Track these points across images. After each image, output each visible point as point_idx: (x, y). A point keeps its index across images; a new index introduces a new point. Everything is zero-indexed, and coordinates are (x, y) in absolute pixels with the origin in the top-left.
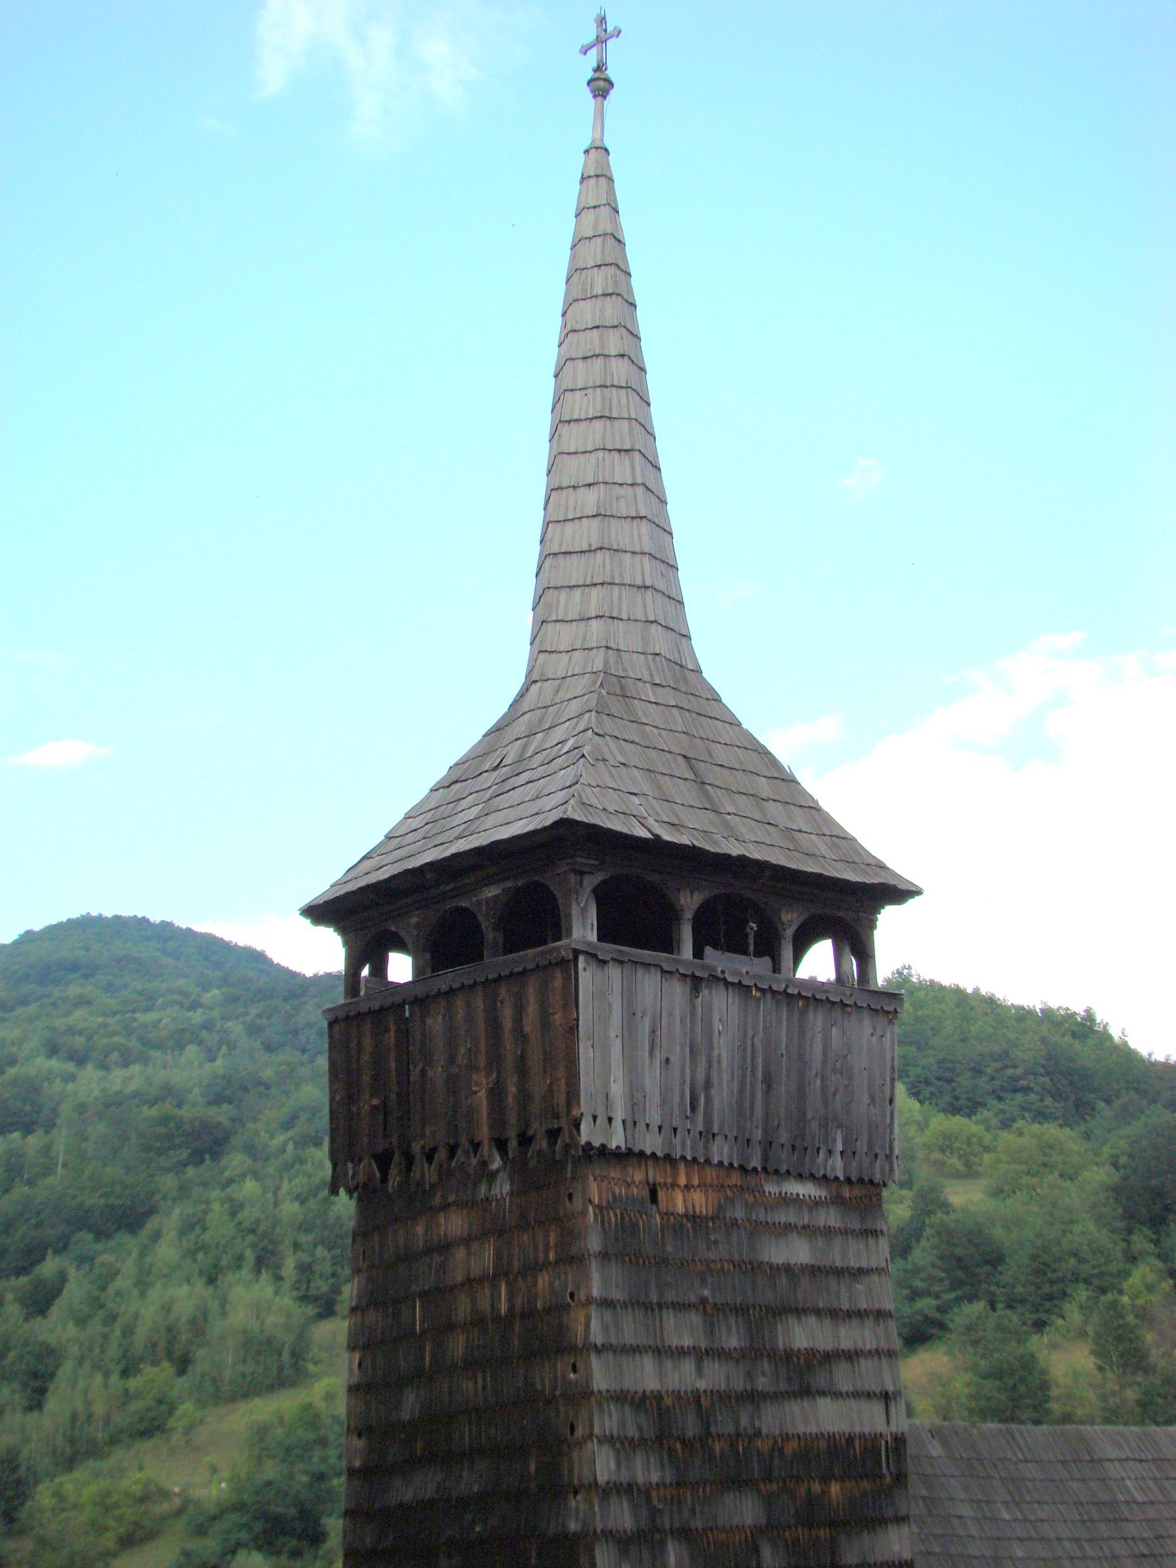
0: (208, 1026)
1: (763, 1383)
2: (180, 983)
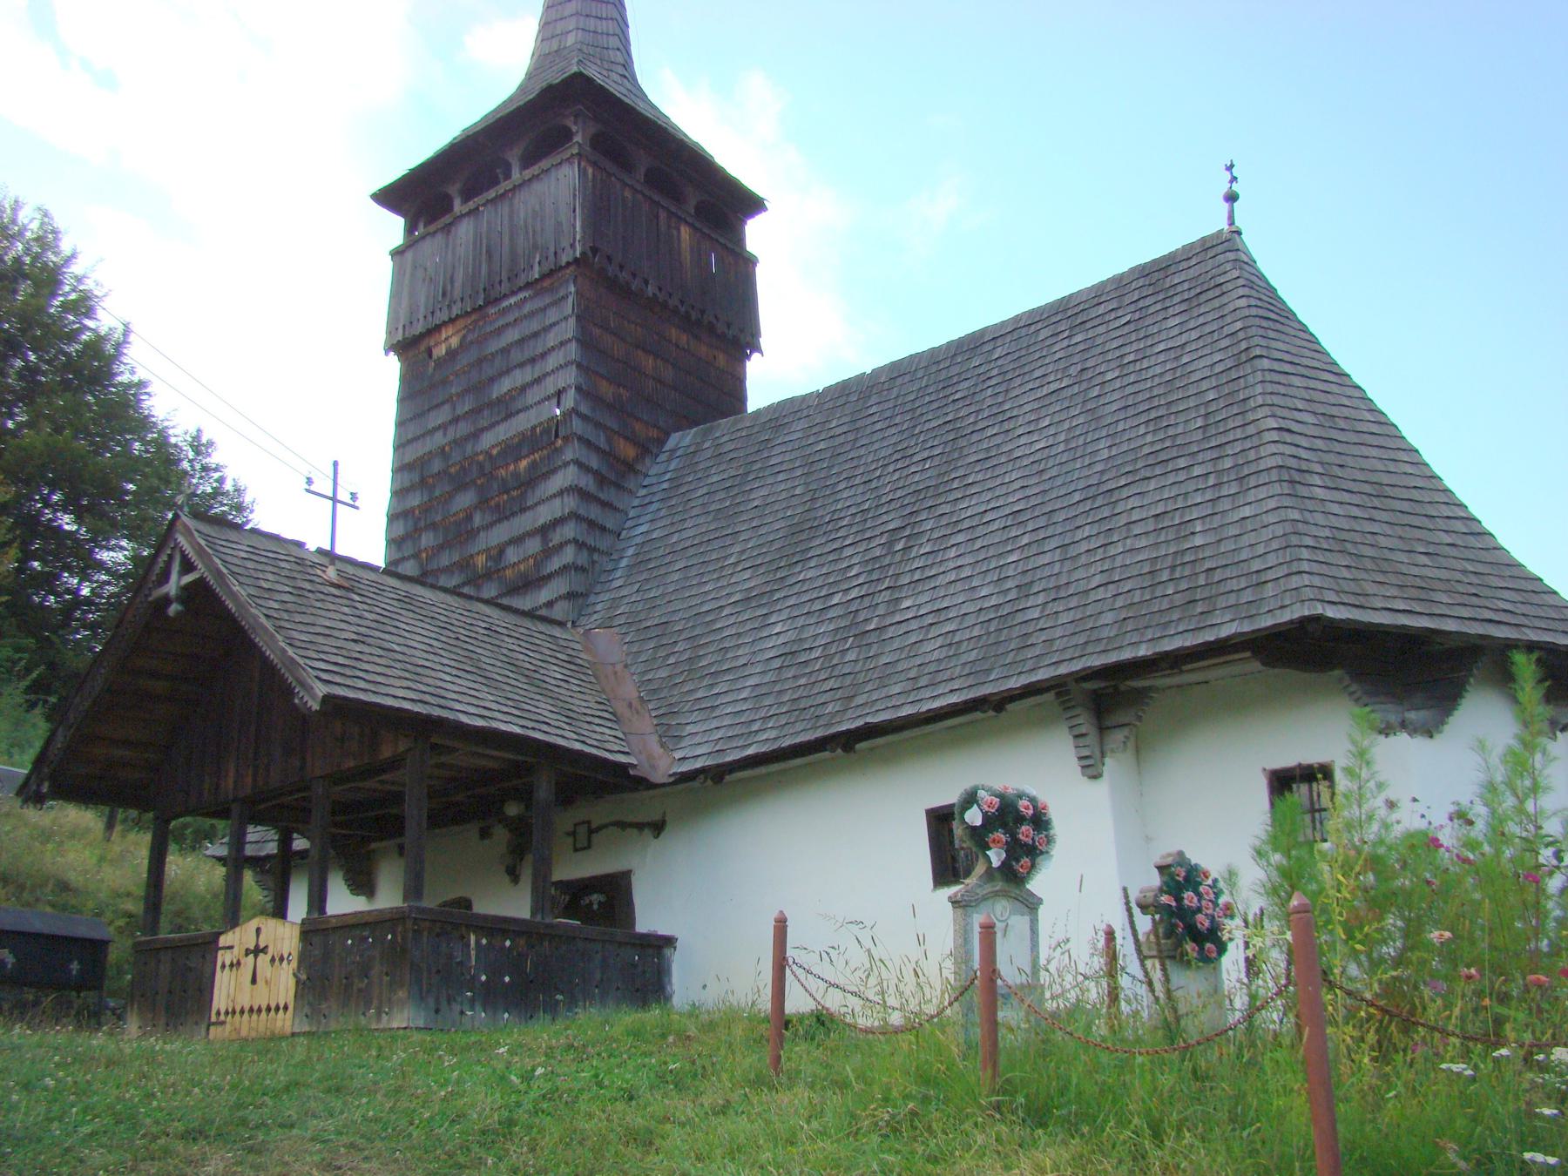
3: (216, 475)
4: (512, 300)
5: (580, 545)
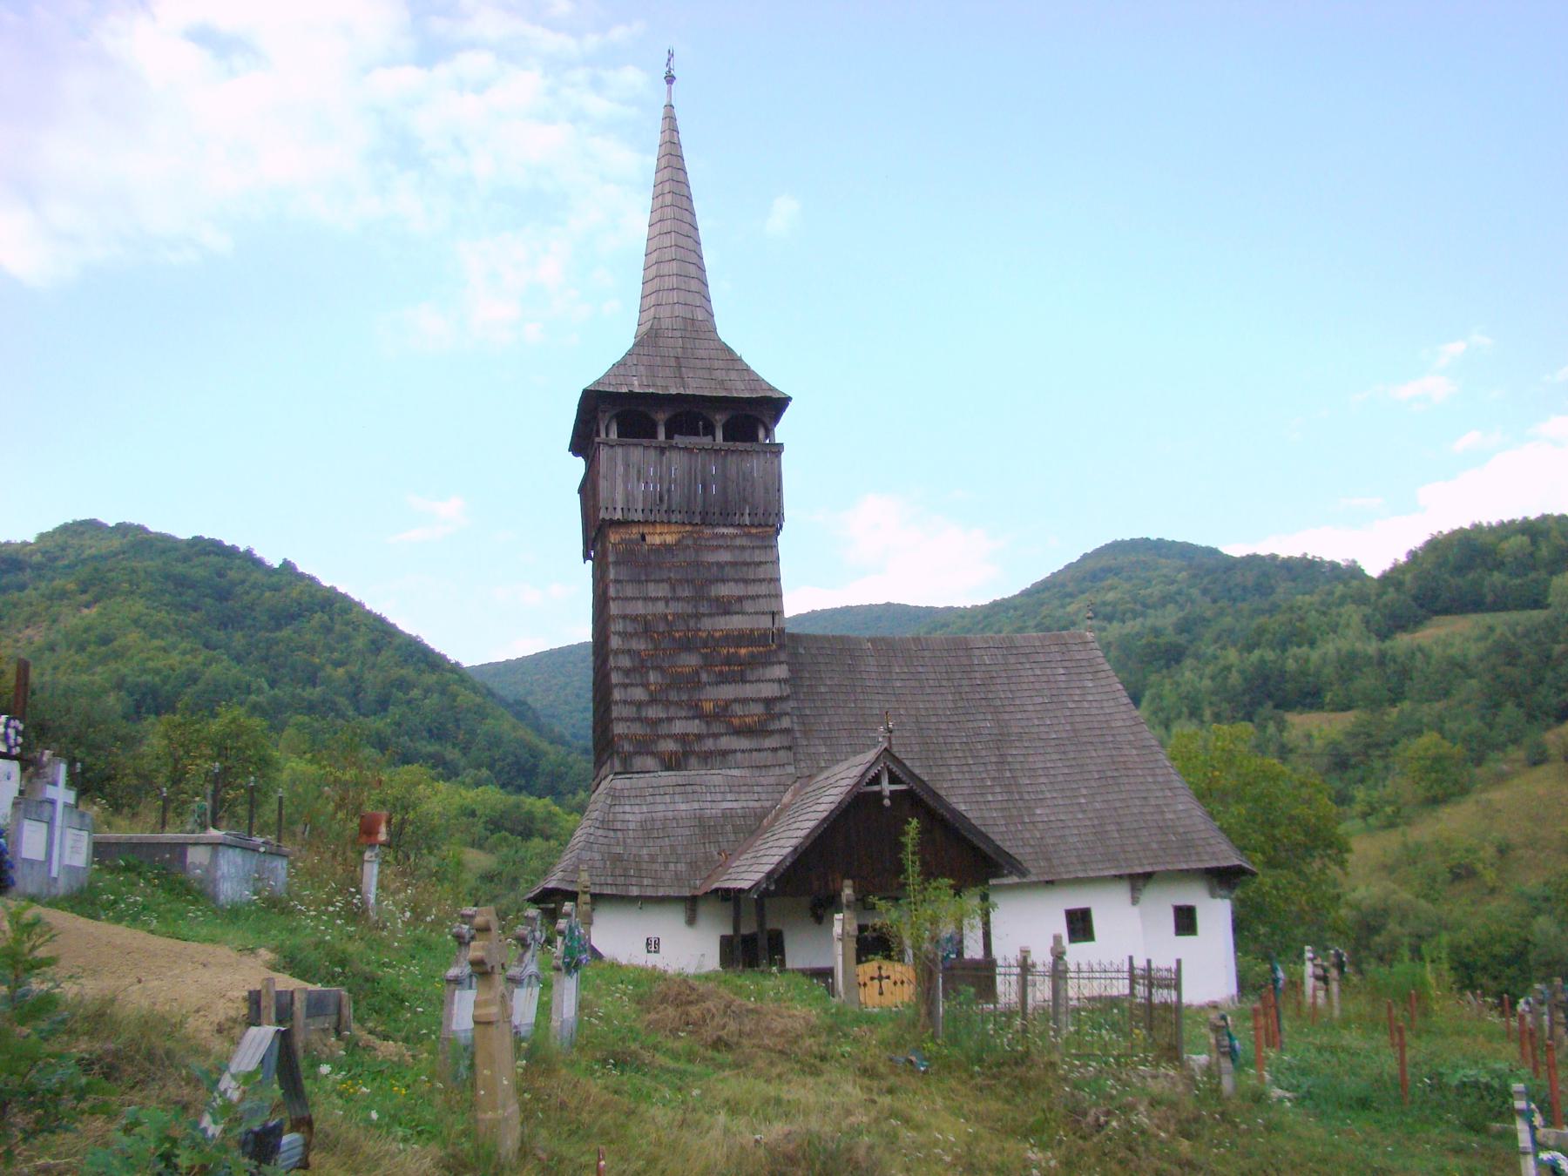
0: (1180, 593)
1: (702, 610)
2: (1165, 571)
4: (725, 531)
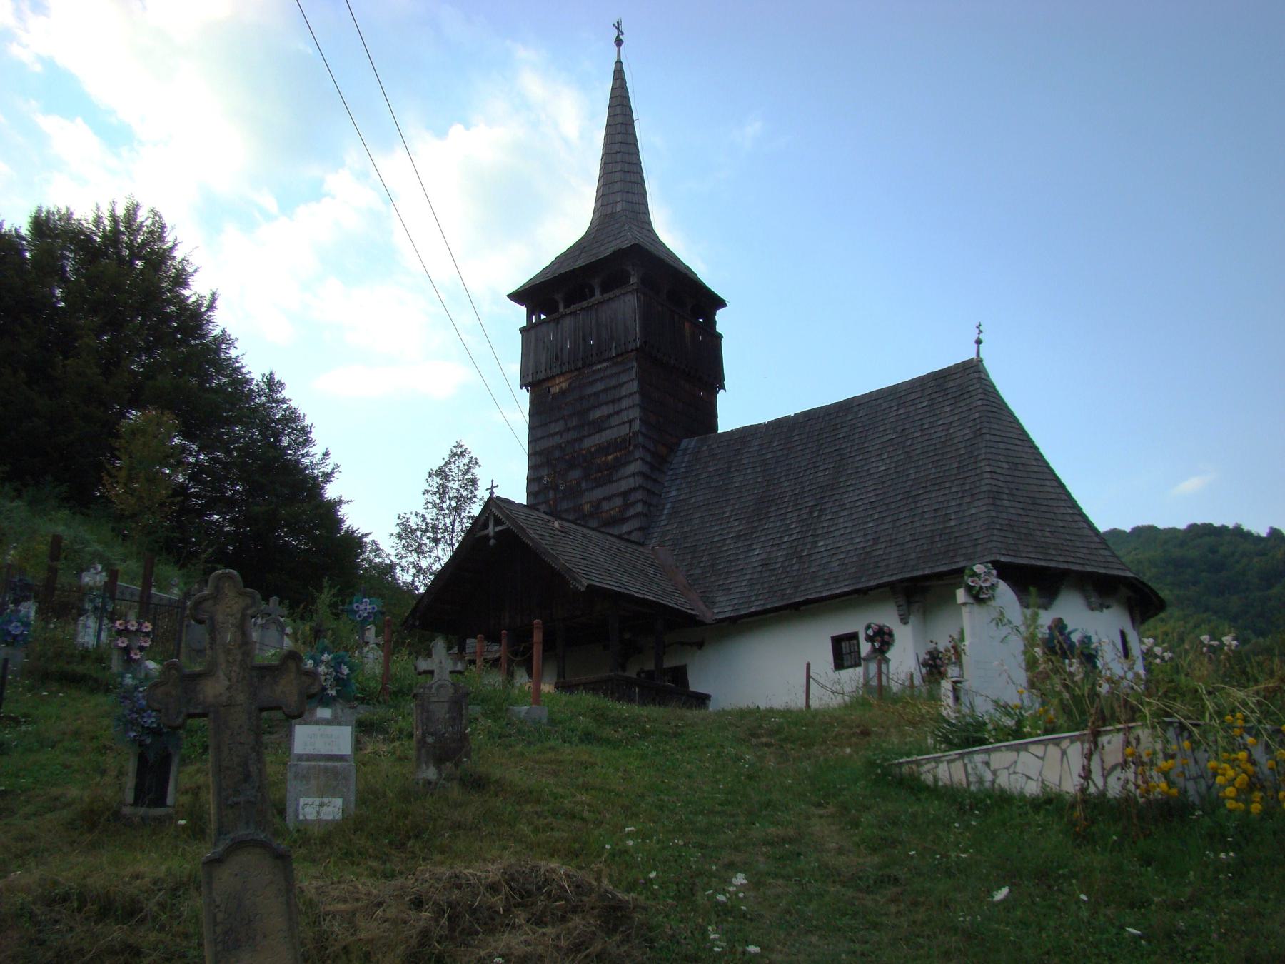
3: (285, 406)
4: (599, 367)
5: (644, 502)
